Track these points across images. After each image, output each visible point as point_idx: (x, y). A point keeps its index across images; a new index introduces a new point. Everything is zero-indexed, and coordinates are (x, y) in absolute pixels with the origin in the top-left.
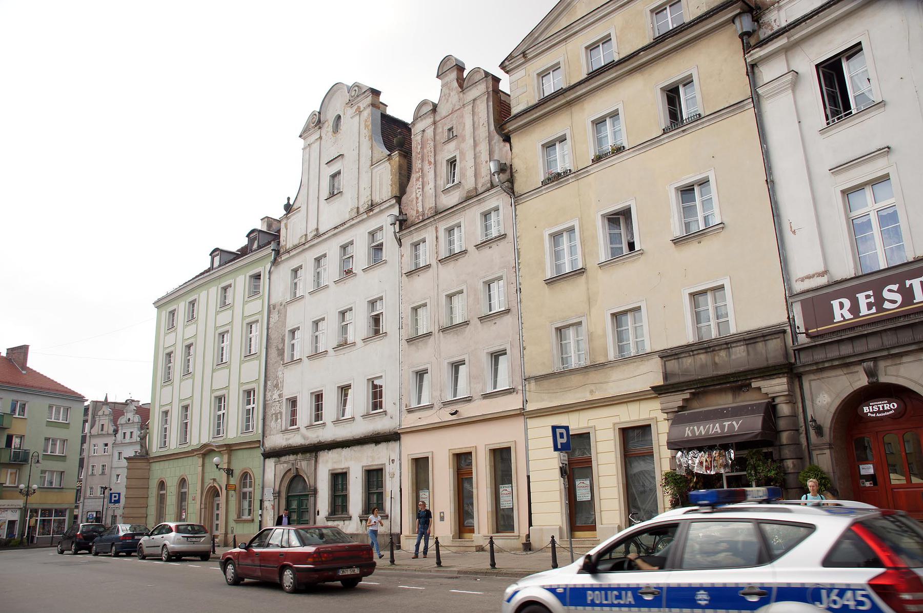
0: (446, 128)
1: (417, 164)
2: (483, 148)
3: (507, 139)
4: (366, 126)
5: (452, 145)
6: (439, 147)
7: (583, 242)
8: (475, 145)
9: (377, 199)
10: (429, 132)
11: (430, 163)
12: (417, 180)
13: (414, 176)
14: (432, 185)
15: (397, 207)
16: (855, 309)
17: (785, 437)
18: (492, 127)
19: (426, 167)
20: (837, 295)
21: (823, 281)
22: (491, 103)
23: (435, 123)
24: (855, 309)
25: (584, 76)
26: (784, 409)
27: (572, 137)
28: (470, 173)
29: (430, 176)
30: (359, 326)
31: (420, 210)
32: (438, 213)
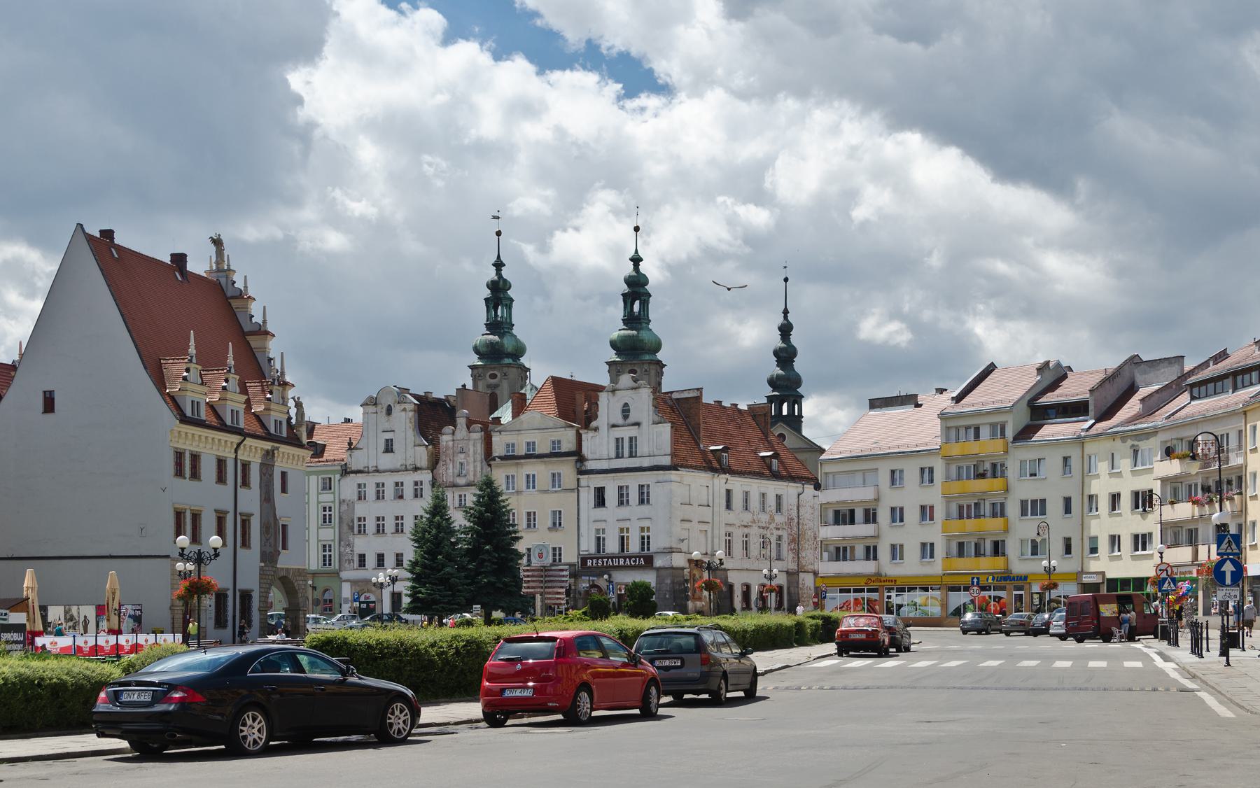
0: (460, 446)
1: (443, 457)
2: (479, 464)
3: (490, 466)
4: (410, 422)
5: (462, 456)
6: (455, 455)
7: (518, 519)
8: (475, 461)
9: (418, 465)
10: (451, 444)
11: (450, 460)
12: (443, 465)
13: (441, 463)
14: (451, 471)
15: (431, 474)
16: (592, 563)
17: (572, 596)
18: (483, 457)
19: (448, 461)
20: (589, 558)
21: (587, 553)
22: (483, 445)
23: (453, 440)
24: (592, 563)
25: (524, 454)
26: (573, 587)
27: (517, 476)
28: (472, 474)
29: (451, 466)
30: (390, 525)
31: (445, 480)
32: (454, 485)
